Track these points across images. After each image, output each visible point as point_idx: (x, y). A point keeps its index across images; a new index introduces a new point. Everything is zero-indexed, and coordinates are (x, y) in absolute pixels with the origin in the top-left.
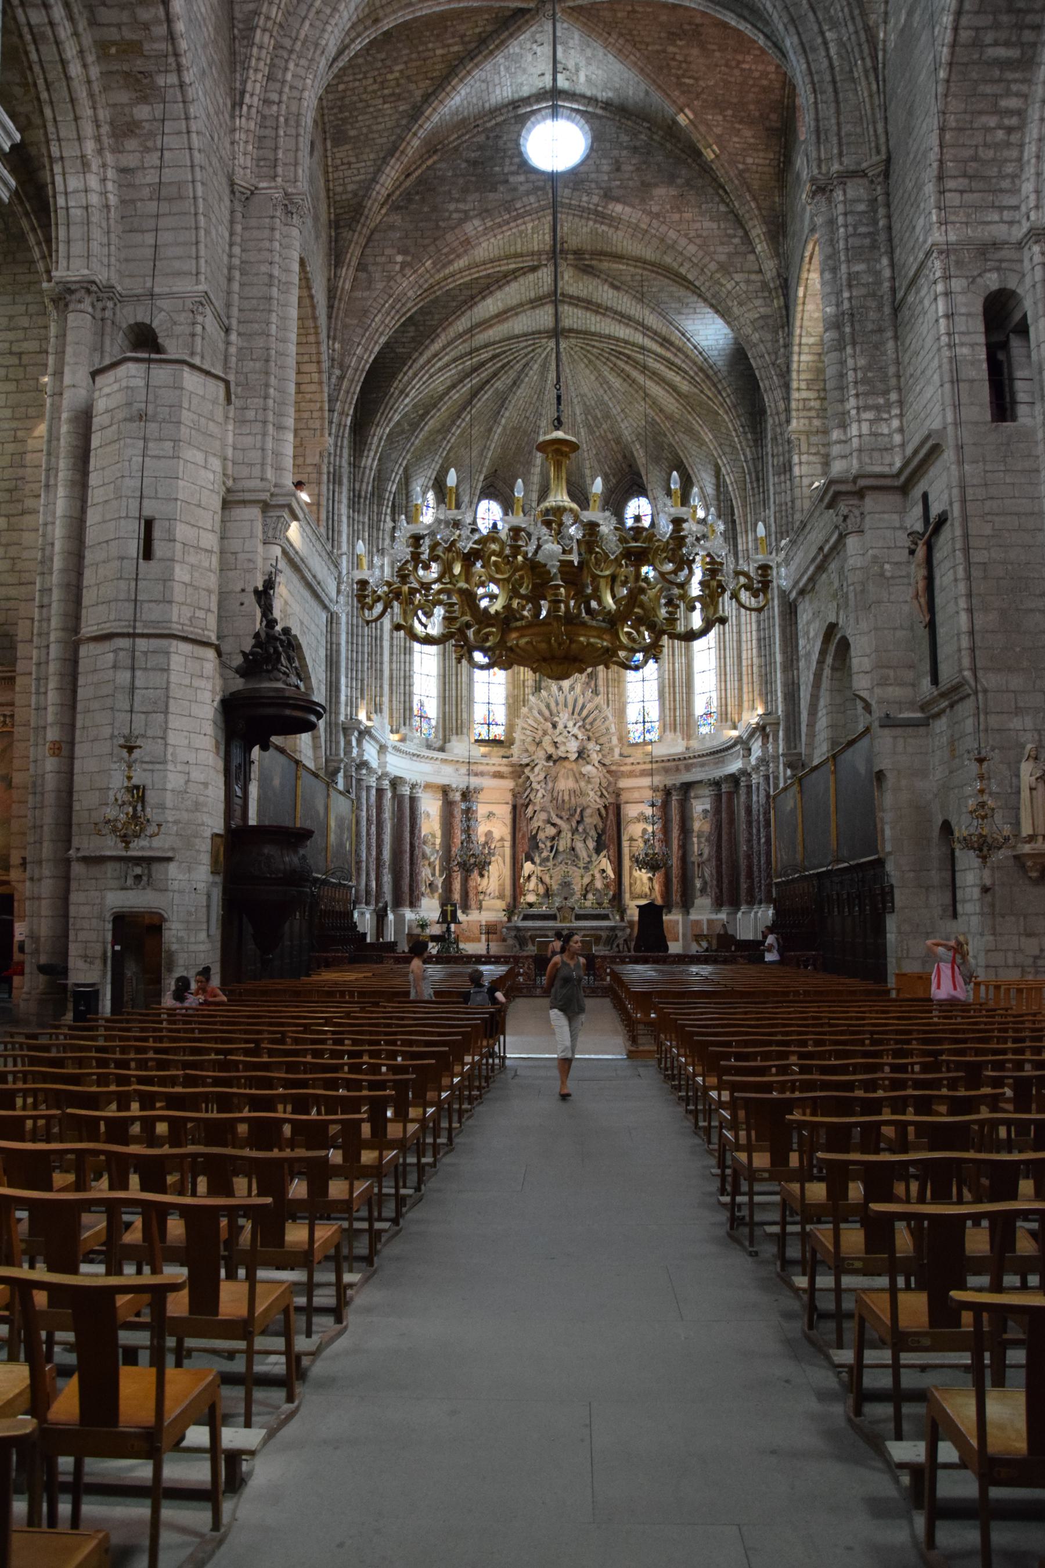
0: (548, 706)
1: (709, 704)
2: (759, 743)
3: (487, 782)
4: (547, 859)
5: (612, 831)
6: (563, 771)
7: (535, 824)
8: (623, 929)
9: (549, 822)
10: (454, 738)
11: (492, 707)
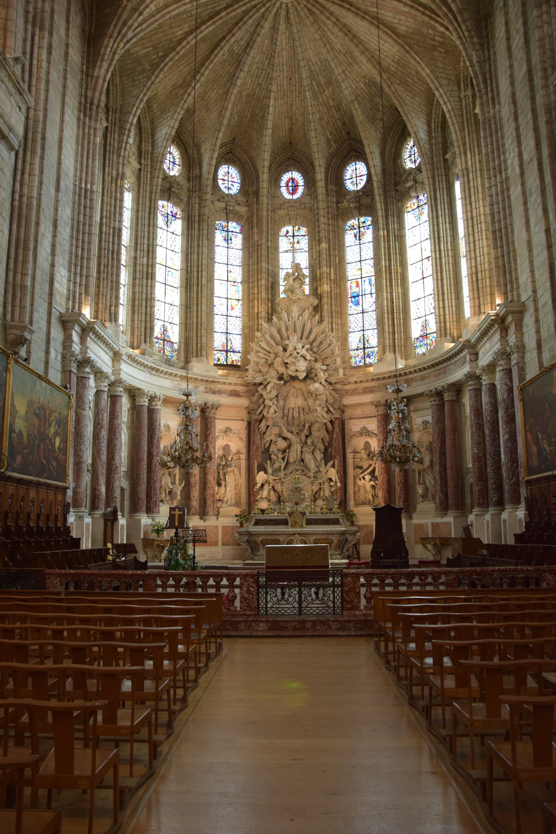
0: (279, 331)
1: (425, 326)
2: (497, 337)
3: (224, 400)
4: (279, 470)
5: (337, 444)
6: (293, 390)
7: (268, 438)
8: (354, 533)
9: (280, 436)
10: (194, 359)
11: (230, 336)
